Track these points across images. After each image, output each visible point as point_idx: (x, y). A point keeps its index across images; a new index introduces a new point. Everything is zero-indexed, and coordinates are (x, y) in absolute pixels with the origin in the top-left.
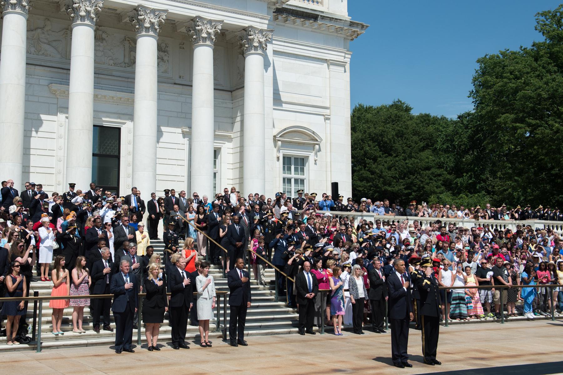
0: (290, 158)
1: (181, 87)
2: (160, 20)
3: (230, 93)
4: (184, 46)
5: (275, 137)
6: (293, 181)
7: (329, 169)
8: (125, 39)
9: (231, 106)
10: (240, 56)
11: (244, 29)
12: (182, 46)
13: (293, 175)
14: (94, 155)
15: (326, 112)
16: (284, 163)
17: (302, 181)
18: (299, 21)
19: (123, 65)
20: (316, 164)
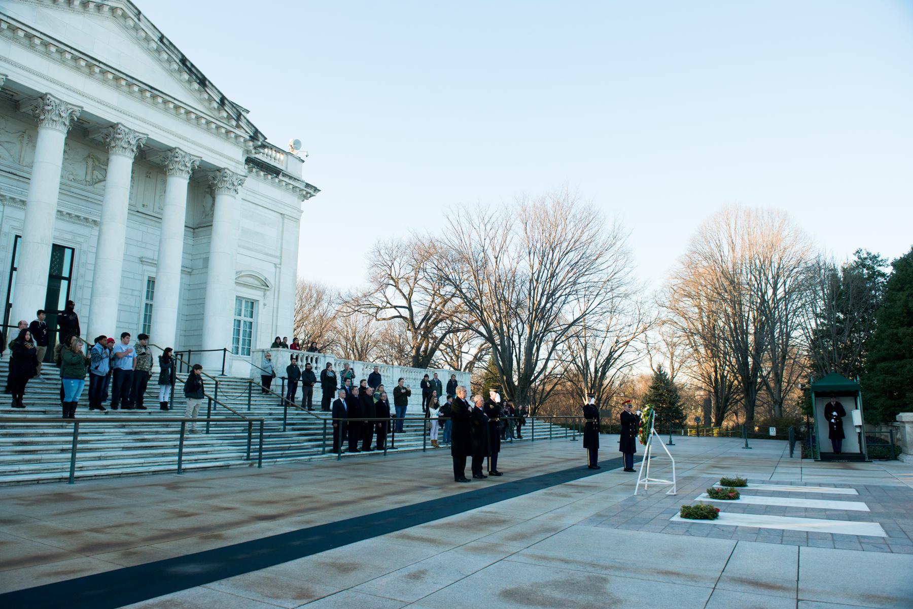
1: (144, 216)
2: (139, 143)
3: (192, 230)
4: (151, 176)
6: (242, 323)
7: (275, 315)
8: (89, 156)
9: (191, 242)
10: (208, 196)
11: (218, 170)
12: (149, 175)
13: (242, 318)
15: (277, 261)
16: (236, 305)
18: (262, 173)
19: (84, 182)
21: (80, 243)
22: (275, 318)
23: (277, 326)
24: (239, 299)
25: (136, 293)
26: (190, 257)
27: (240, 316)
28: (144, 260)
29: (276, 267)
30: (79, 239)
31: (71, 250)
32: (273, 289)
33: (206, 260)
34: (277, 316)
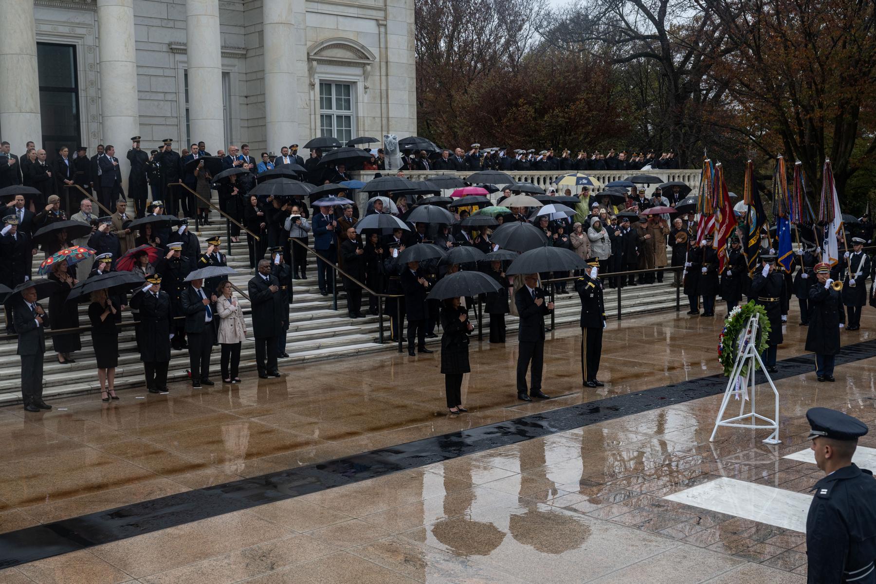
0: (330, 85)
5: (308, 54)
13: (334, 111)
14: (41, 89)
15: (380, 15)
16: (321, 93)
17: (348, 118)
20: (366, 92)
21: (81, 37)
22: (384, 106)
23: (388, 118)
24: (326, 86)
25: (170, 97)
26: (242, 31)
27: (331, 109)
28: (173, 46)
29: (379, 25)
30: (80, 31)
31: (71, 49)
32: (377, 60)
33: (261, 33)
34: (387, 103)
